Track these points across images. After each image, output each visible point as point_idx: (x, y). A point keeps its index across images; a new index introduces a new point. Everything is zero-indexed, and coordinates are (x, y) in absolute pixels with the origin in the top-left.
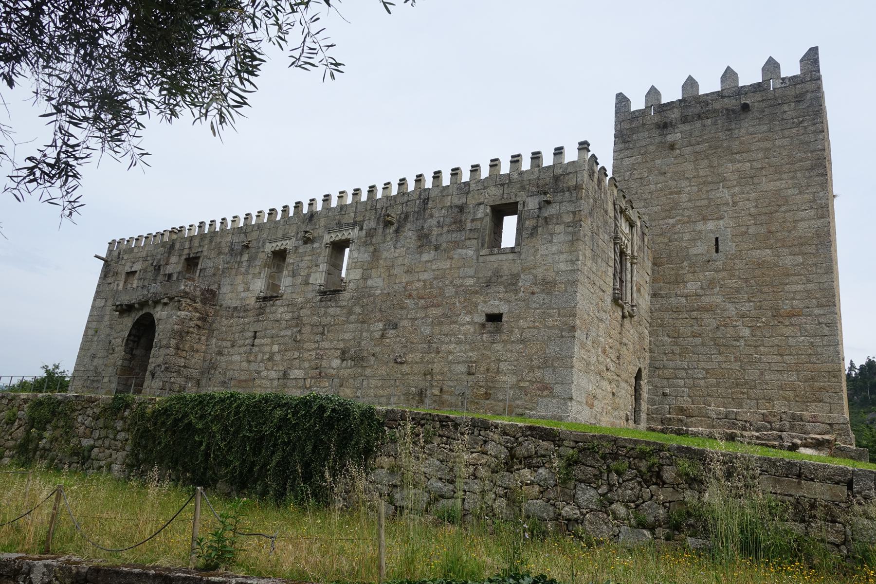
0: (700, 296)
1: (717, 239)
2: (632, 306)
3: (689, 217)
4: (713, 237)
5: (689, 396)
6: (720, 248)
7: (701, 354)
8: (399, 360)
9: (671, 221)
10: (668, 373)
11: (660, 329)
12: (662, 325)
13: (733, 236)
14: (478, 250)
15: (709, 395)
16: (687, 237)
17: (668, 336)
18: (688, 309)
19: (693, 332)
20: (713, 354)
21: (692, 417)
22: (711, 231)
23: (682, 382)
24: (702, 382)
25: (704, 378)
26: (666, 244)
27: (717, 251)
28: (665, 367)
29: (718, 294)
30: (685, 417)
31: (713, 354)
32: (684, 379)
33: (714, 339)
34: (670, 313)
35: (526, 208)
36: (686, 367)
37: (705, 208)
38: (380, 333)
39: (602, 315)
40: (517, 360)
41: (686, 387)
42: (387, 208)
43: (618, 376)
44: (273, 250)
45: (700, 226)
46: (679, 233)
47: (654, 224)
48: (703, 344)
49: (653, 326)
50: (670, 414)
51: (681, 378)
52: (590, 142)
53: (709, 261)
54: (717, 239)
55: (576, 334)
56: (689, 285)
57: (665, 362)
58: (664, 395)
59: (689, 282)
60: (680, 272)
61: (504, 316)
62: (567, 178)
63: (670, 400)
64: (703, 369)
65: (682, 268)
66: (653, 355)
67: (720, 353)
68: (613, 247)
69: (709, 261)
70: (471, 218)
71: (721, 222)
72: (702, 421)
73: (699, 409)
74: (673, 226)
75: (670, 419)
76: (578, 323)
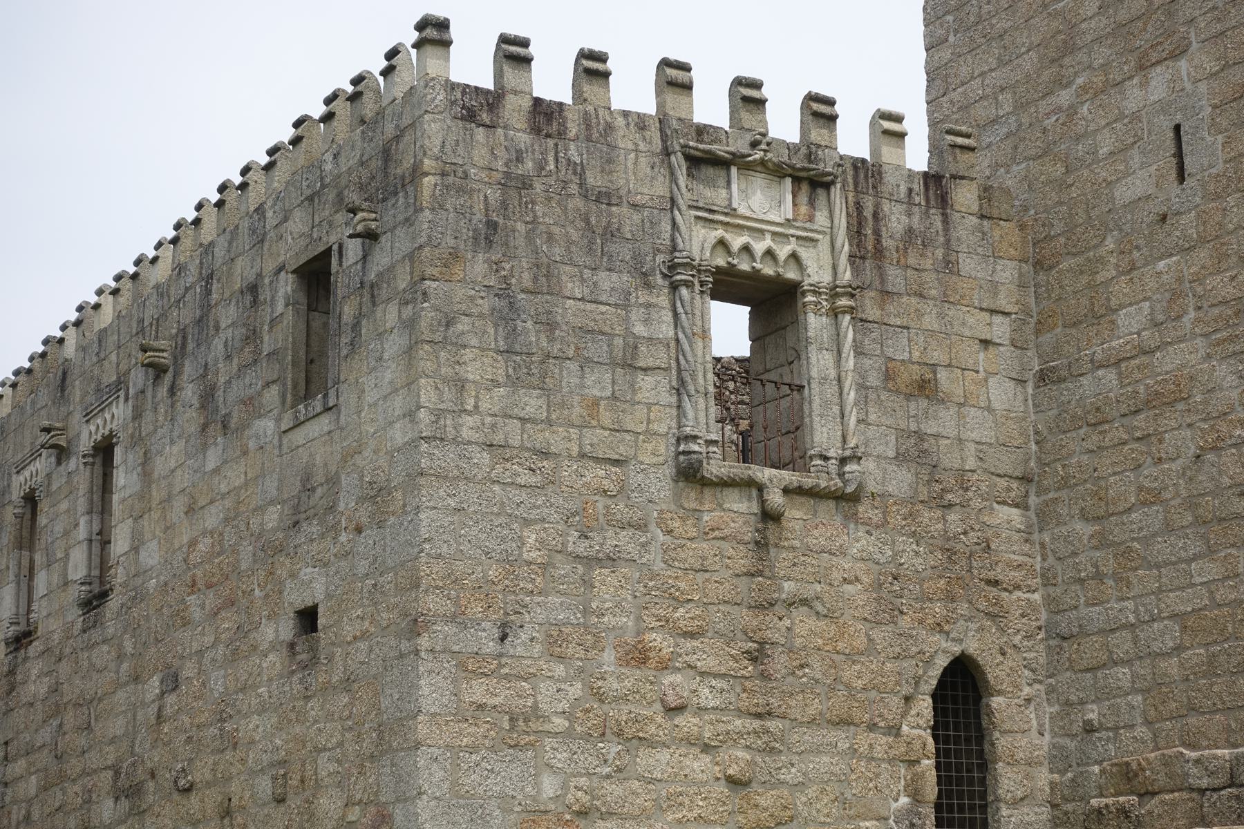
0: (1151, 352)
1: (1177, 128)
2: (843, 461)
3: (1105, 67)
4: (1166, 124)
5: (1148, 722)
6: (1187, 160)
7: (1166, 564)
8: (182, 783)
9: (1064, 97)
10: (1091, 649)
11: (1064, 494)
12: (1064, 483)
13: (1215, 107)
14: (278, 420)
15: (1193, 709)
16: (1106, 144)
17: (1084, 516)
18: (1124, 409)
19: (1140, 489)
20: (1194, 558)
21: (1154, 794)
22: (1163, 107)
23: (1123, 673)
24: (1172, 667)
25: (1179, 649)
26: (1062, 185)
27: (1181, 177)
28: (1083, 632)
29: (1194, 336)
30: (1134, 799)
31: (1194, 558)
32: (1128, 662)
33: (1191, 503)
34: (1082, 431)
35: (345, 267)
36: (1132, 618)
37: (1140, 24)
38: (155, 707)
39: (625, 541)
40: (341, 744)
41: (1135, 691)
42: (158, 320)
43: (758, 716)
44: (22, 494)
45: (1133, 98)
46: (1085, 135)
47: (1026, 120)
48: (1169, 528)
49: (1047, 490)
50: (1101, 795)
51: (1123, 662)
52: (439, 12)
53: (1164, 218)
54: (1177, 128)
55: (424, 642)
56: (1122, 318)
57: (1083, 610)
58: (1089, 729)
59: (1122, 307)
60: (1100, 278)
61: (321, 610)
62: (401, 146)
63: (1107, 748)
64: (1174, 616)
65: (1101, 260)
66: (1051, 590)
67: (1211, 552)
68: (663, 300)
69: (1164, 218)
70: (268, 319)
71: (1183, 64)
72: (1174, 804)
73: (1166, 762)
74: (1072, 111)
75: (1099, 811)
76: (433, 603)
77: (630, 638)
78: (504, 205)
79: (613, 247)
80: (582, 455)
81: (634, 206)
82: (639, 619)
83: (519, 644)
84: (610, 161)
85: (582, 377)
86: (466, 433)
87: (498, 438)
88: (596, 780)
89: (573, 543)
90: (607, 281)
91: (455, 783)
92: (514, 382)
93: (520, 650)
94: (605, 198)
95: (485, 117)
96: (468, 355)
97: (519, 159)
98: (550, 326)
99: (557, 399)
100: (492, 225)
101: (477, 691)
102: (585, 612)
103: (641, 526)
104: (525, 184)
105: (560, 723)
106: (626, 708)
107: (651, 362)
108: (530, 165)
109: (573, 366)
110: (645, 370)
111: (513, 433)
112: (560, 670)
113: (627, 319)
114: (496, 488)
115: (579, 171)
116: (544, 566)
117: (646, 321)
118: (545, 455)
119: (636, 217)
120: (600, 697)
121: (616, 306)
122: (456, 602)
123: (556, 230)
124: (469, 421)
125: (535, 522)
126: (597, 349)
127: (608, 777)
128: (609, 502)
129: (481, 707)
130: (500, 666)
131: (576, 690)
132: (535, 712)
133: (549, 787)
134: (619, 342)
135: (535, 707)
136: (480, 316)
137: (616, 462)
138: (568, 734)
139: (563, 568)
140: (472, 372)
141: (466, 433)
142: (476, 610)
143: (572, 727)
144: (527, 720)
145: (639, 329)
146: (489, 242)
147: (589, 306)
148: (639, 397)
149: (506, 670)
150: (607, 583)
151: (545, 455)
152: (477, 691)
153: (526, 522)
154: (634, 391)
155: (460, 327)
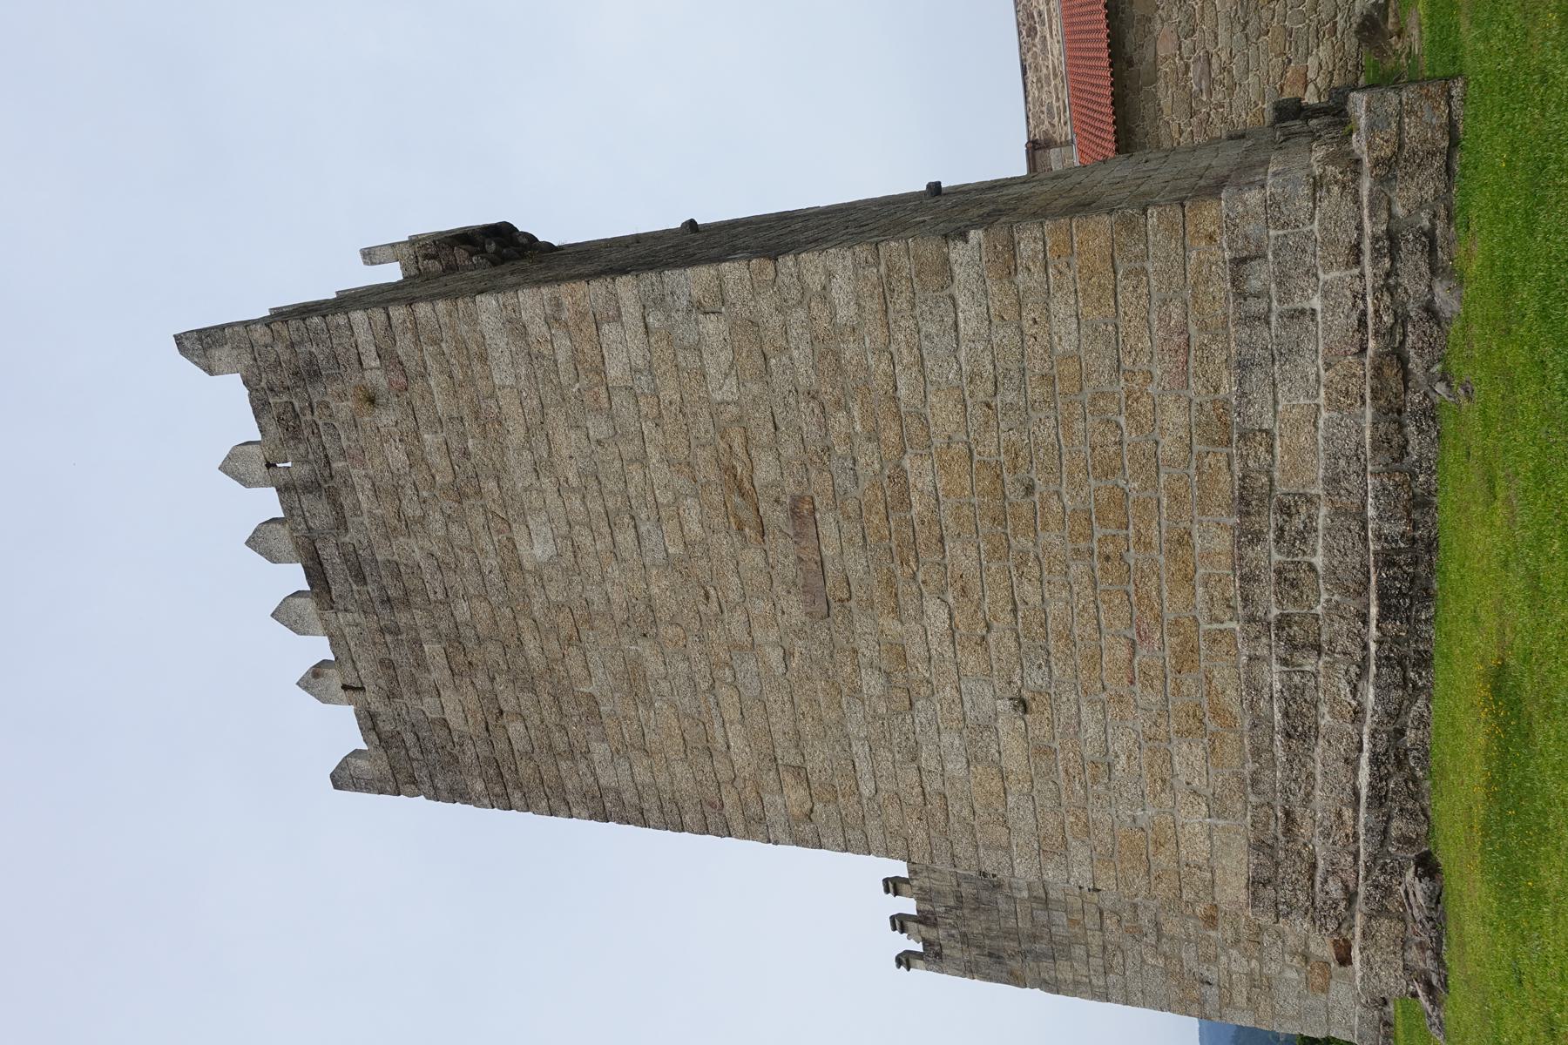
52: (894, 964)
77: (1201, 924)
78: (977, 947)
79: (984, 900)
80: (1101, 930)
81: (959, 885)
82: (1188, 916)
83: (1213, 977)
84: (939, 893)
85: (1058, 925)
86: (1101, 983)
87: (1102, 970)
88: (1285, 949)
89: (1152, 939)
90: (1003, 906)
91: (1293, 1018)
92: (1069, 958)
93: (1215, 976)
94: (959, 898)
95: (937, 948)
96: (1060, 976)
97: (953, 936)
98: (1034, 938)
99: (1074, 941)
100: (990, 955)
101: (1240, 1000)
102: (1190, 942)
103: (1135, 906)
104: (964, 935)
105: (1254, 963)
106: (1242, 930)
107: (1041, 891)
108: (953, 932)
109: (1054, 929)
110: (1046, 894)
111: (1096, 962)
112: (1223, 959)
113: (1021, 899)
114: (1128, 973)
115: (949, 909)
116: (1166, 958)
117: (1020, 890)
118: (1105, 948)
119: (964, 885)
120: (1237, 941)
121: (1015, 903)
122: (1193, 1002)
123: (984, 926)
124: (1094, 981)
125: (1142, 957)
126: (1042, 916)
127: (1283, 942)
128: (1124, 920)
129: (1249, 999)
130: (1225, 987)
131: (1234, 953)
132: (1250, 974)
133: (1291, 974)
134: (1034, 905)
135: (1246, 974)
136: (1038, 966)
137: (1101, 914)
138: (1260, 960)
139: (1165, 948)
140: (1070, 977)
141: (1101, 983)
142: (1195, 994)
143: (1256, 958)
144: (1255, 980)
145: (1025, 894)
146: (999, 957)
147: (1019, 916)
148: (1062, 898)
149: (1227, 985)
150: (1167, 928)
151: (1105, 948)
152: (1240, 1000)
153: (1143, 961)
154: (1060, 901)
155: (1047, 977)
